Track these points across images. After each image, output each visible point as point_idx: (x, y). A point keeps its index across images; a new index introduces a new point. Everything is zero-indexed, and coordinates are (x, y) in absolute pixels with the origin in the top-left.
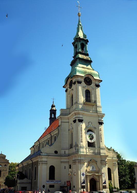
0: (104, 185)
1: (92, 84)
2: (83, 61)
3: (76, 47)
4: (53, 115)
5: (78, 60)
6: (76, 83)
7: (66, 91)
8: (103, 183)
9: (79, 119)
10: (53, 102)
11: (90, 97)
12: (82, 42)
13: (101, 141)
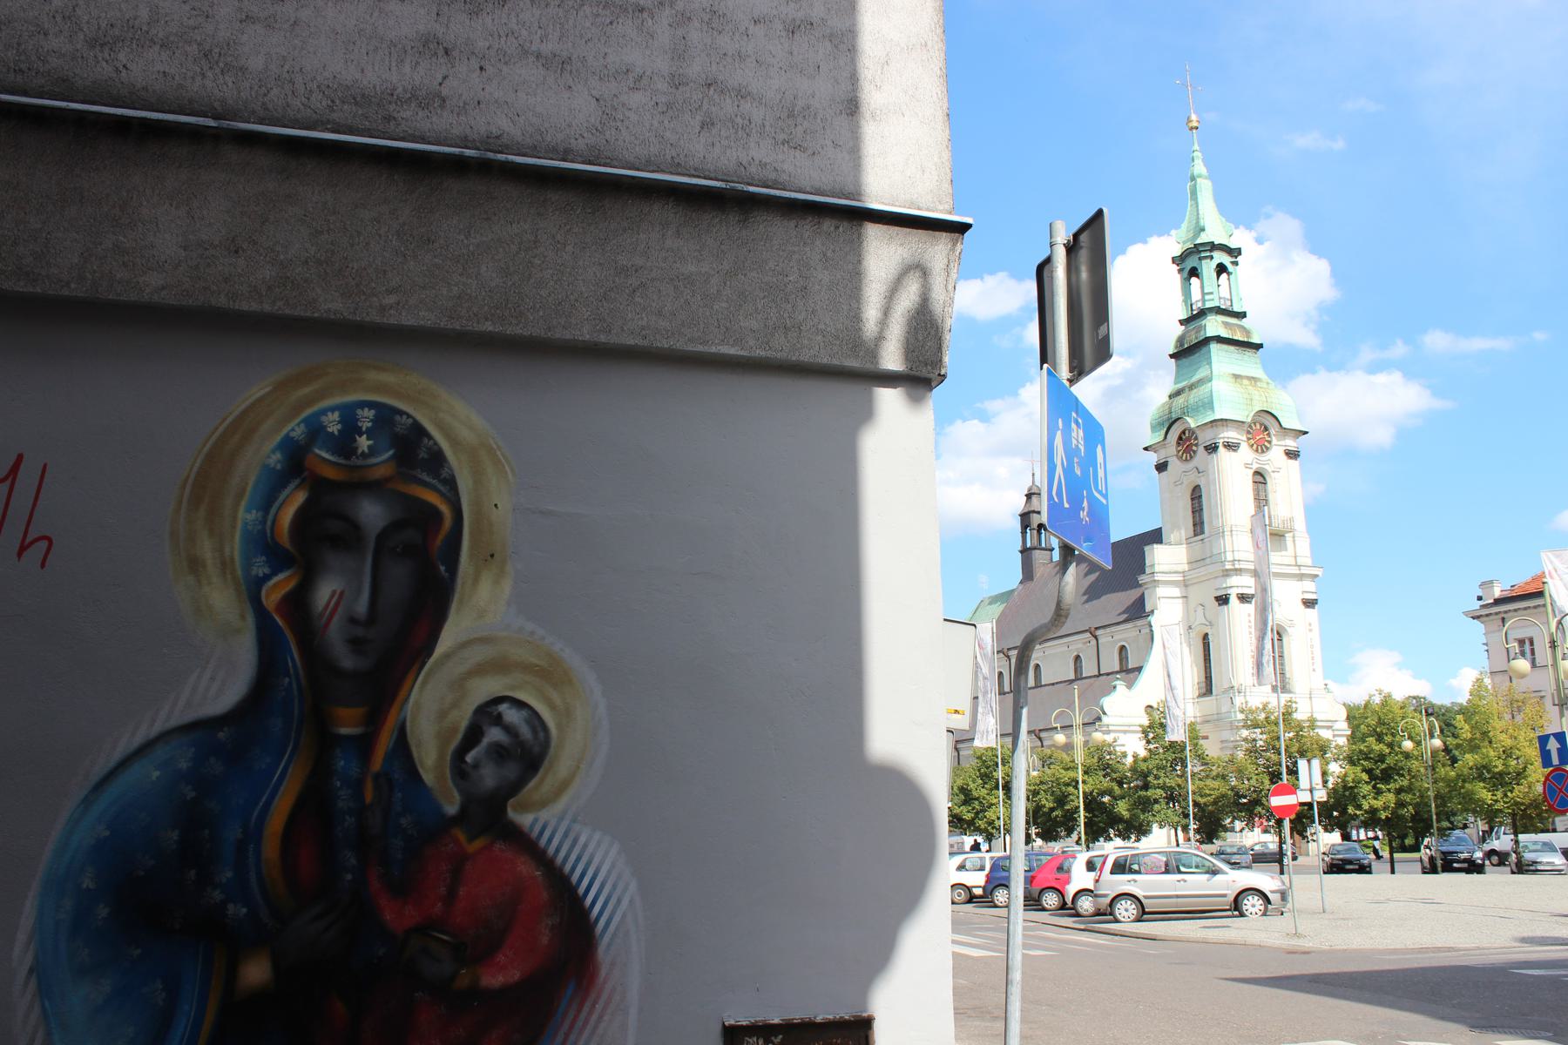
1: (1274, 448)
2: (1232, 348)
10: (1033, 475)
12: (1220, 257)
13: (1314, 670)
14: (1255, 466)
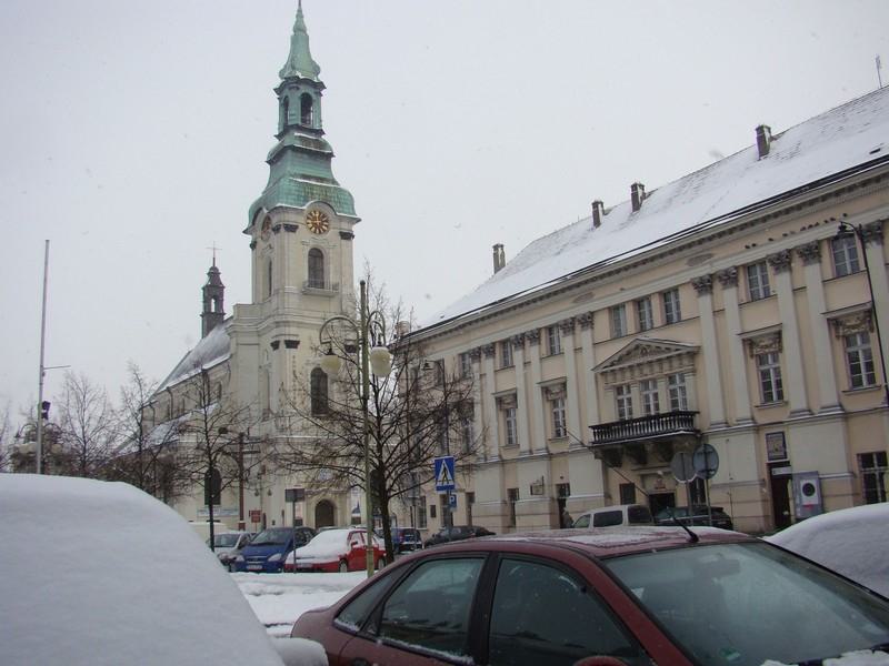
0: (356, 515)
2: (305, 156)
3: (285, 104)
4: (213, 301)
5: (289, 152)
6: (282, 230)
7: (253, 246)
8: (354, 512)
9: (287, 338)
11: (322, 270)
12: (304, 89)
14: (312, 244)
